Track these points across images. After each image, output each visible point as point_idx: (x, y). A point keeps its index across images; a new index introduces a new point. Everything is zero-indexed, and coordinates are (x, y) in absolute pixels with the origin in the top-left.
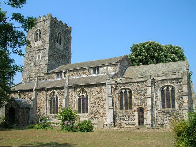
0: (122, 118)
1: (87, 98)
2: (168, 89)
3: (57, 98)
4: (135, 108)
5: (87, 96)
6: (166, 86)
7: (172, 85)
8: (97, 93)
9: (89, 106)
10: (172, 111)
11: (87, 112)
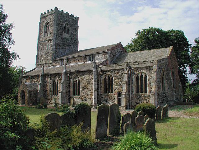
0: (106, 100)
1: (79, 83)
2: (142, 76)
3: (58, 82)
4: (115, 91)
5: (79, 81)
6: (140, 73)
7: (145, 72)
8: (86, 78)
9: (80, 90)
10: (144, 96)
11: (79, 95)
